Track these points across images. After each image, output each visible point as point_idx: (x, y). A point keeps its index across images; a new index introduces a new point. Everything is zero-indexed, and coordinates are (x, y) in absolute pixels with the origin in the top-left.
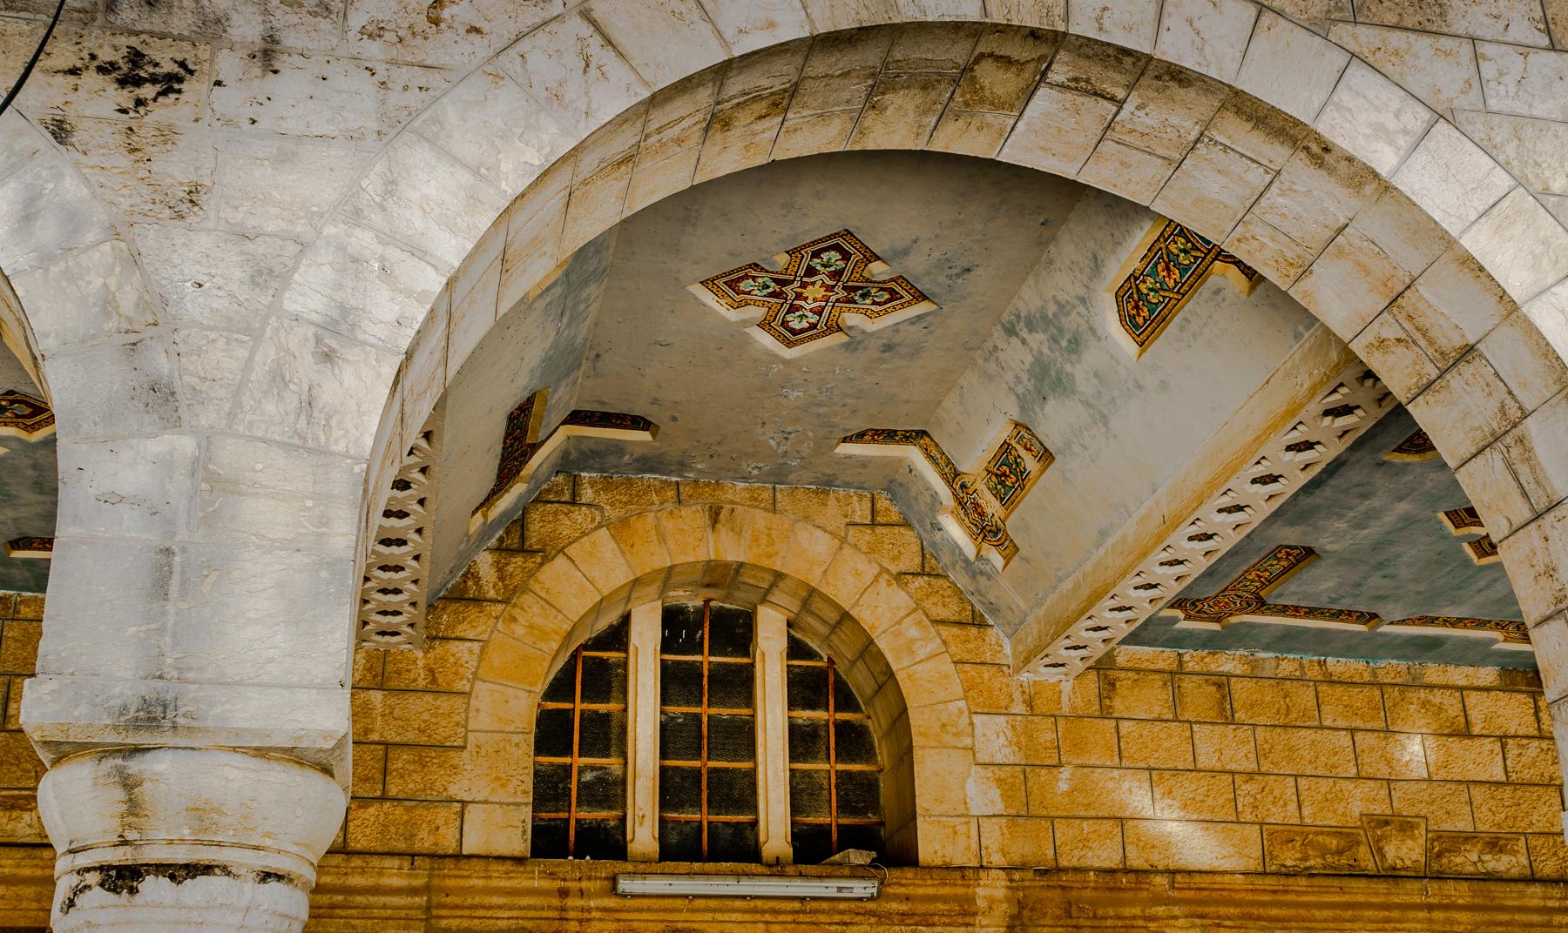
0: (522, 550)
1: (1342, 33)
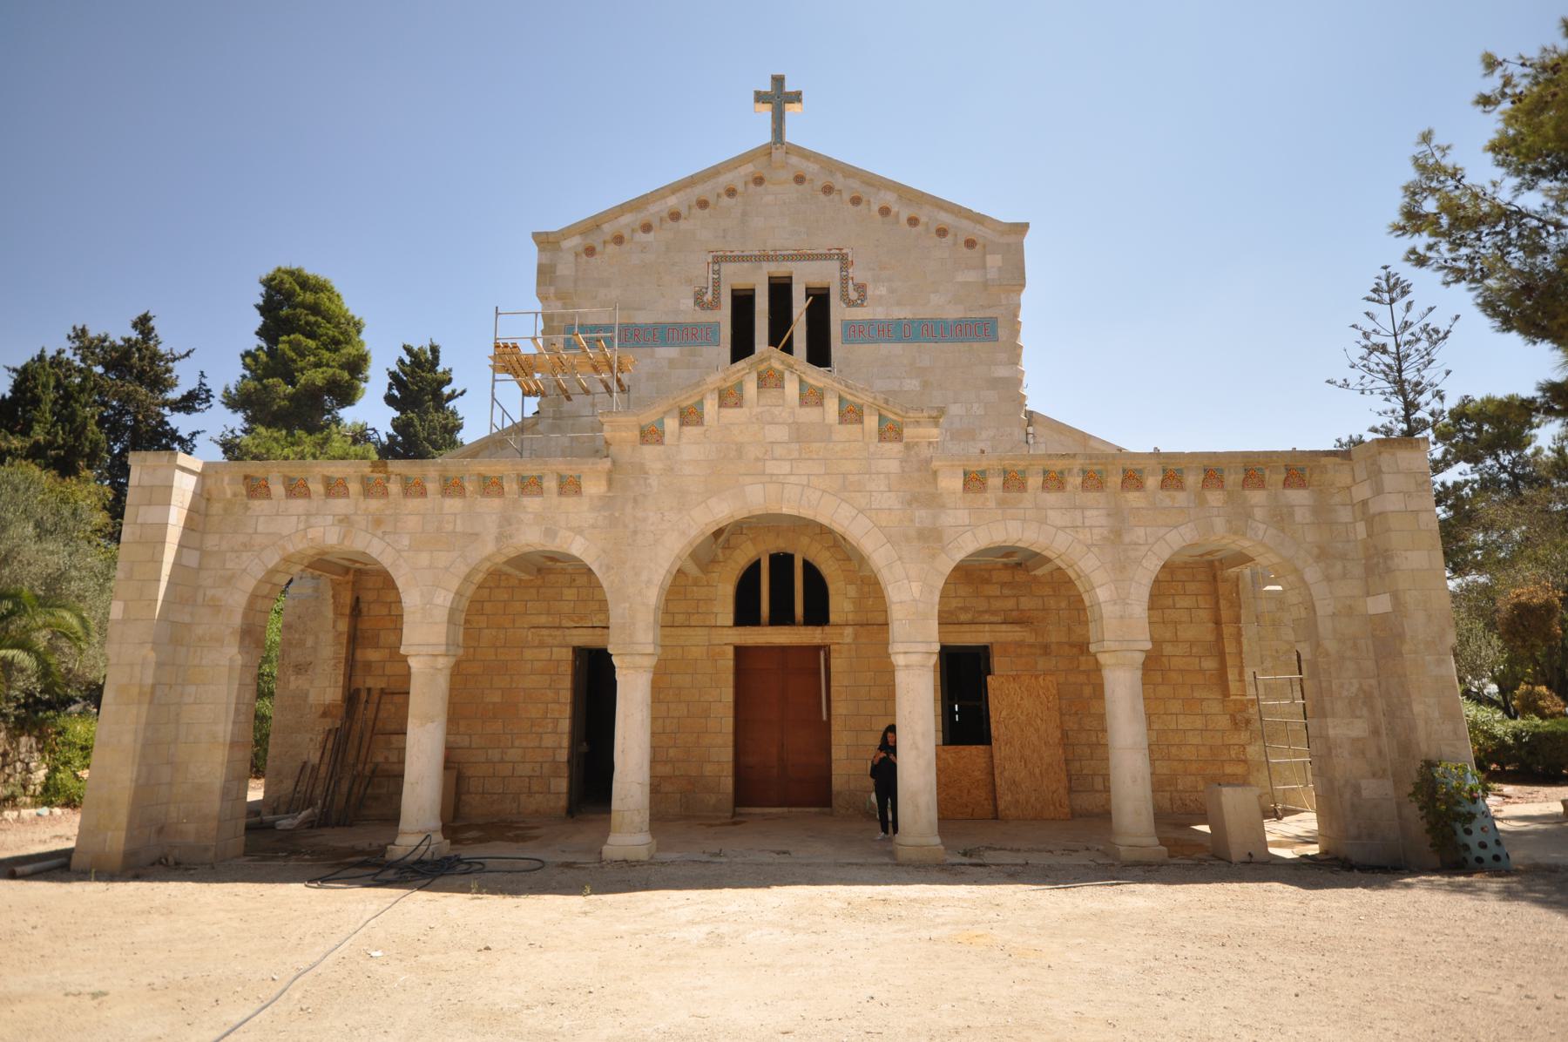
0: (729, 548)
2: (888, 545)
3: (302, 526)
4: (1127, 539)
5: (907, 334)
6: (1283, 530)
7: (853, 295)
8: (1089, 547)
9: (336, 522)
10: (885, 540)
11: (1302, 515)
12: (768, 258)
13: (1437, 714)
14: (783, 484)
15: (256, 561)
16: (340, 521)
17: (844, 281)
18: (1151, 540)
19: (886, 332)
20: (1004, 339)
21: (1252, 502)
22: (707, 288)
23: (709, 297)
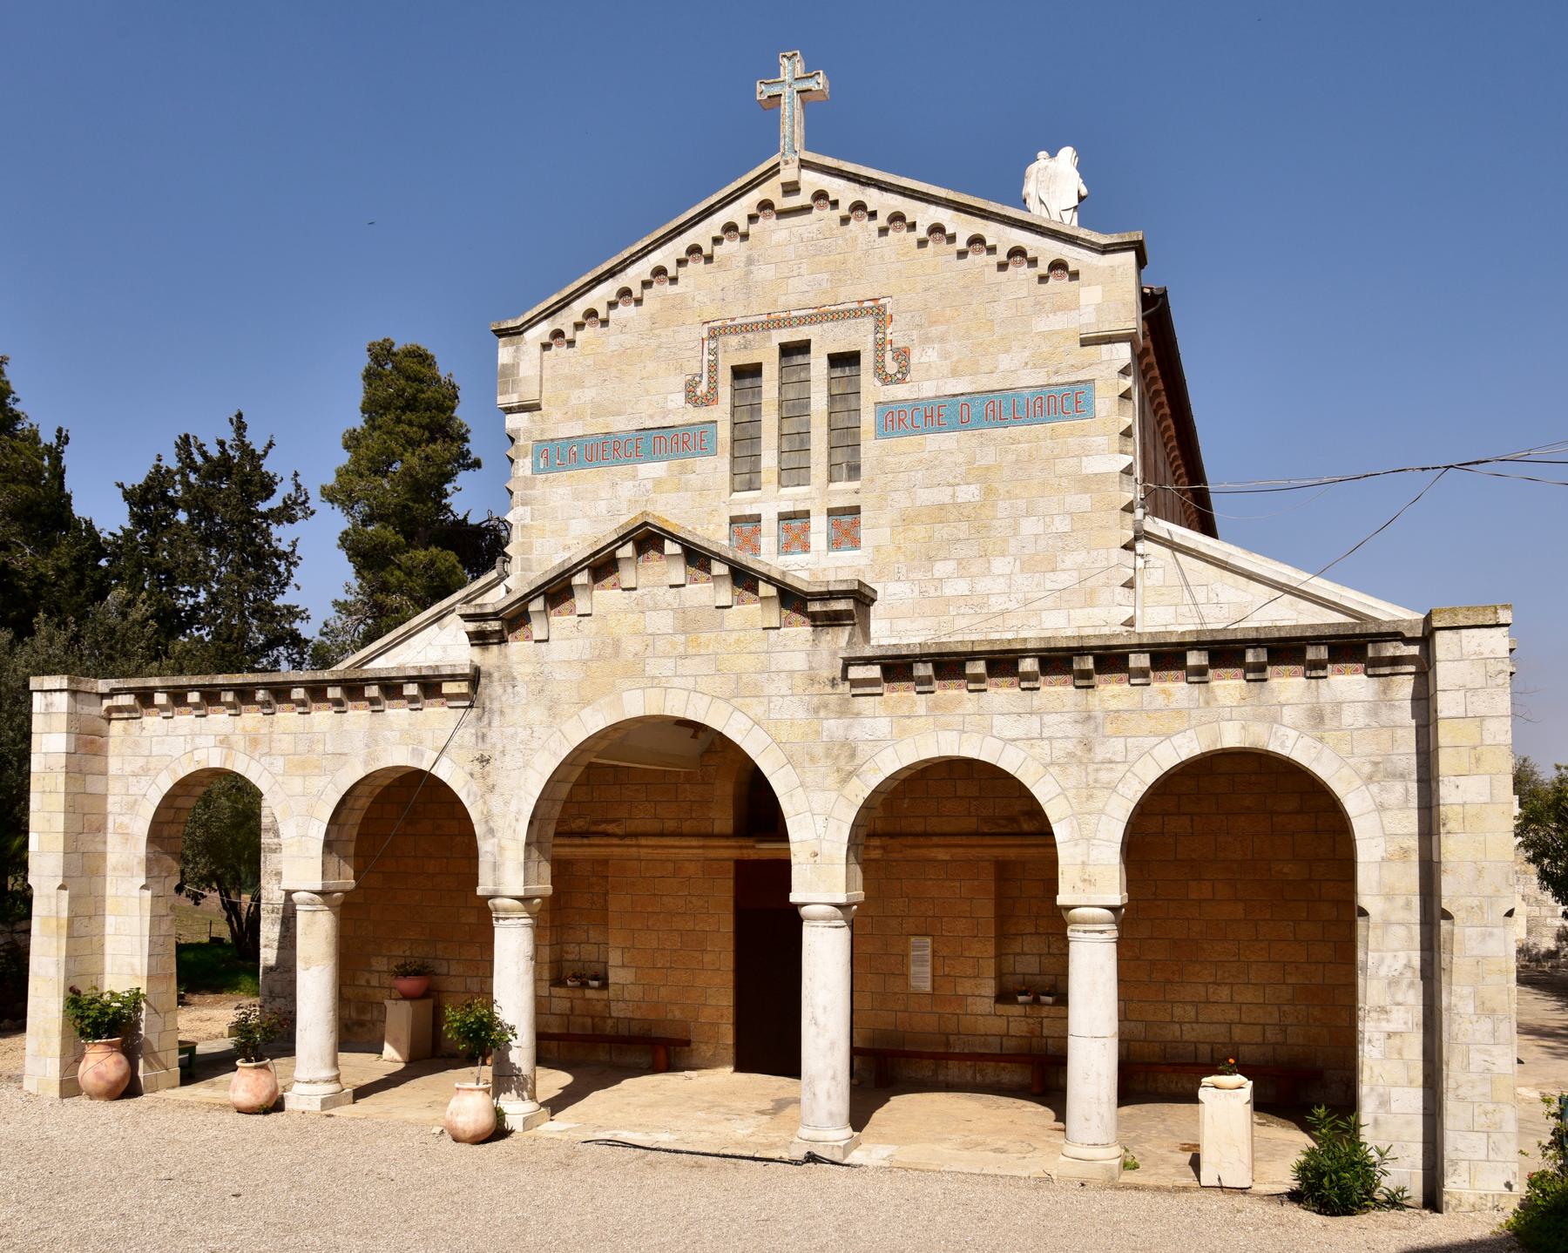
1: (733, 701)
2: (789, 766)
3: (189, 749)
4: (1100, 753)
5: (965, 418)
6: (1321, 739)
7: (891, 367)
8: (1046, 766)
9: (218, 744)
10: (785, 761)
11: (1353, 717)
12: (779, 324)
13: (1471, 1010)
14: (666, 688)
16: (221, 742)
17: (880, 346)
18: (1131, 757)
19: (936, 419)
20: (1104, 414)
21: (1282, 699)
22: (701, 376)
23: (703, 388)
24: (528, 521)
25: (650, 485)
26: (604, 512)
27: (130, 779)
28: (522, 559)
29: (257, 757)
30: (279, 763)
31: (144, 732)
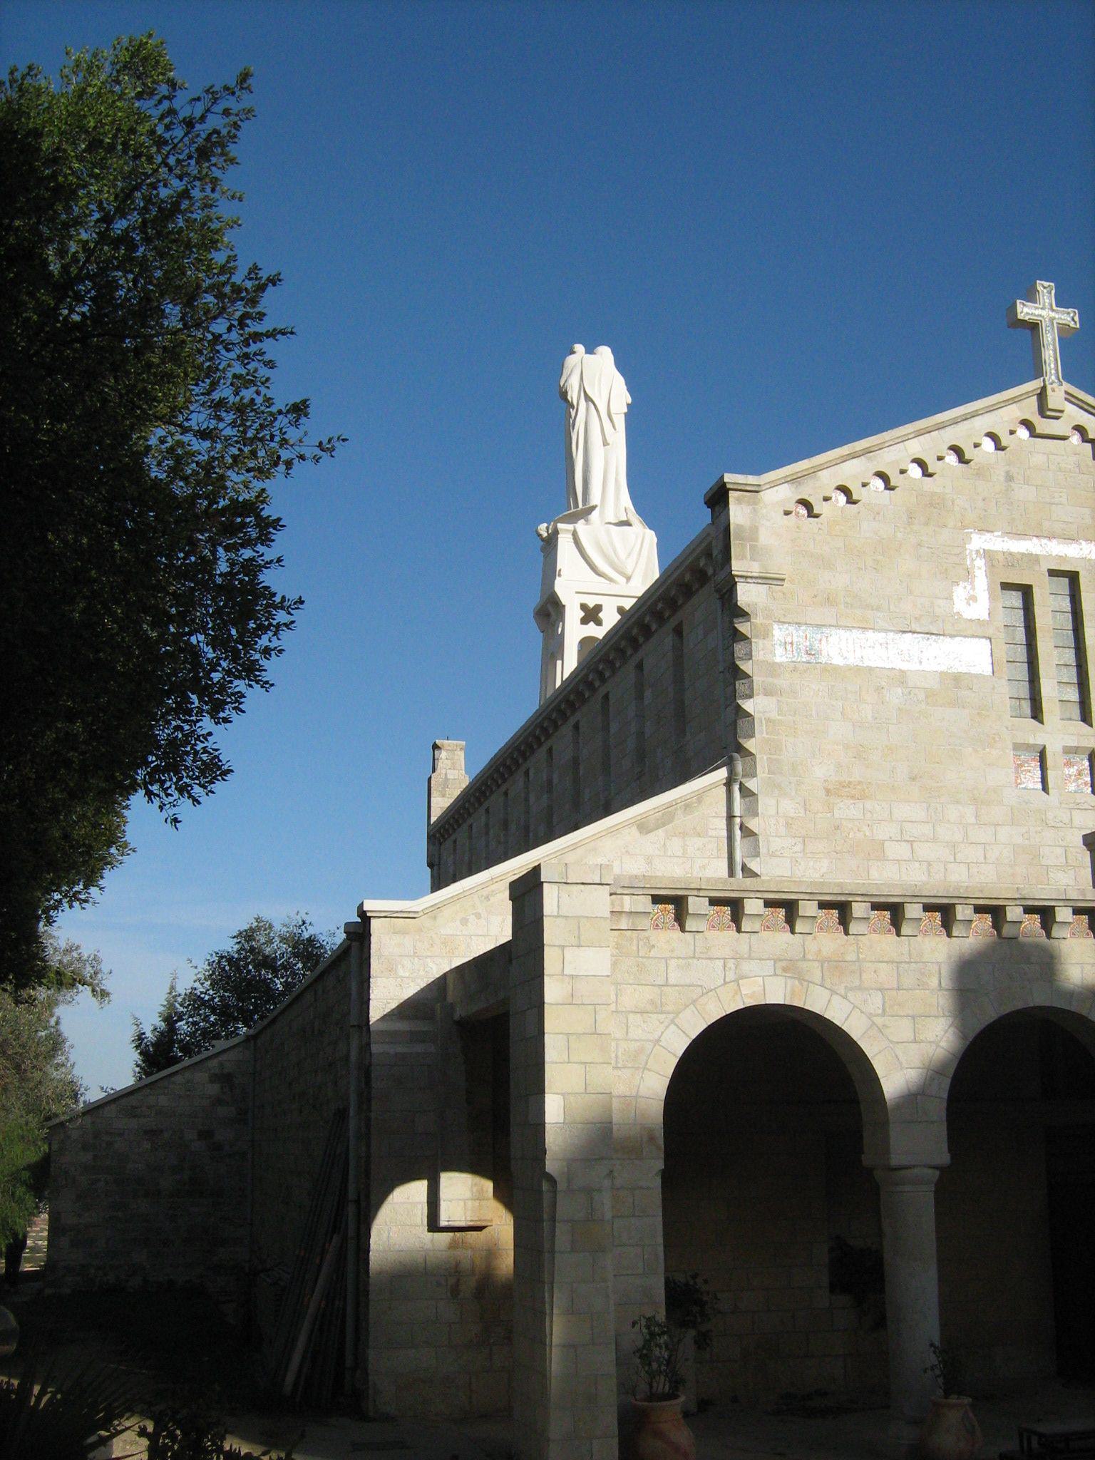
3: (731, 976)
9: (779, 972)
15: (673, 1027)
16: (785, 970)
24: (774, 715)
25: (922, 696)
26: (870, 718)
27: (631, 1016)
28: (770, 760)
29: (843, 992)
30: (876, 1001)
31: (653, 953)
